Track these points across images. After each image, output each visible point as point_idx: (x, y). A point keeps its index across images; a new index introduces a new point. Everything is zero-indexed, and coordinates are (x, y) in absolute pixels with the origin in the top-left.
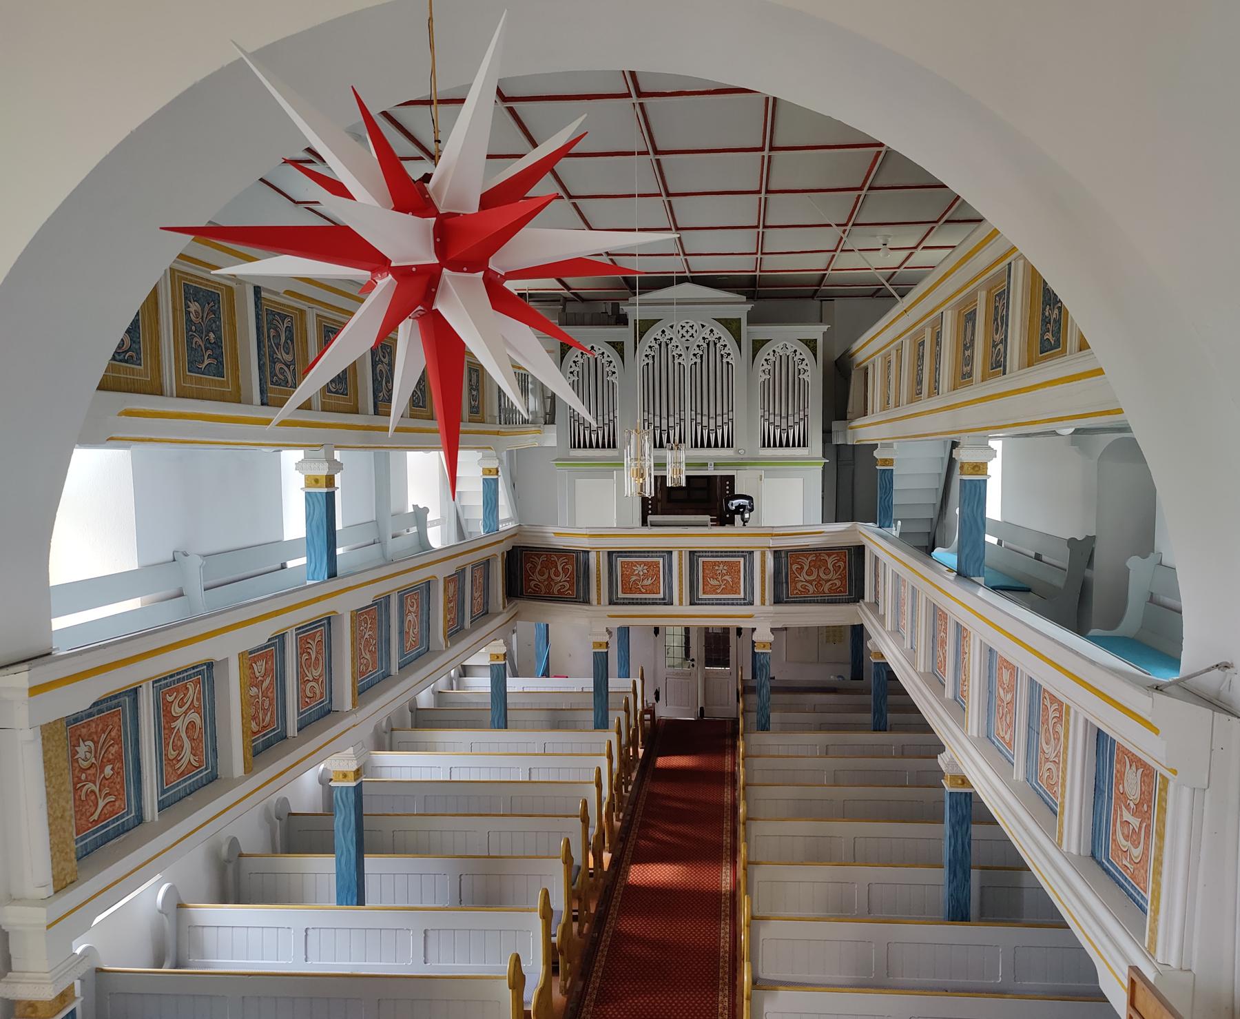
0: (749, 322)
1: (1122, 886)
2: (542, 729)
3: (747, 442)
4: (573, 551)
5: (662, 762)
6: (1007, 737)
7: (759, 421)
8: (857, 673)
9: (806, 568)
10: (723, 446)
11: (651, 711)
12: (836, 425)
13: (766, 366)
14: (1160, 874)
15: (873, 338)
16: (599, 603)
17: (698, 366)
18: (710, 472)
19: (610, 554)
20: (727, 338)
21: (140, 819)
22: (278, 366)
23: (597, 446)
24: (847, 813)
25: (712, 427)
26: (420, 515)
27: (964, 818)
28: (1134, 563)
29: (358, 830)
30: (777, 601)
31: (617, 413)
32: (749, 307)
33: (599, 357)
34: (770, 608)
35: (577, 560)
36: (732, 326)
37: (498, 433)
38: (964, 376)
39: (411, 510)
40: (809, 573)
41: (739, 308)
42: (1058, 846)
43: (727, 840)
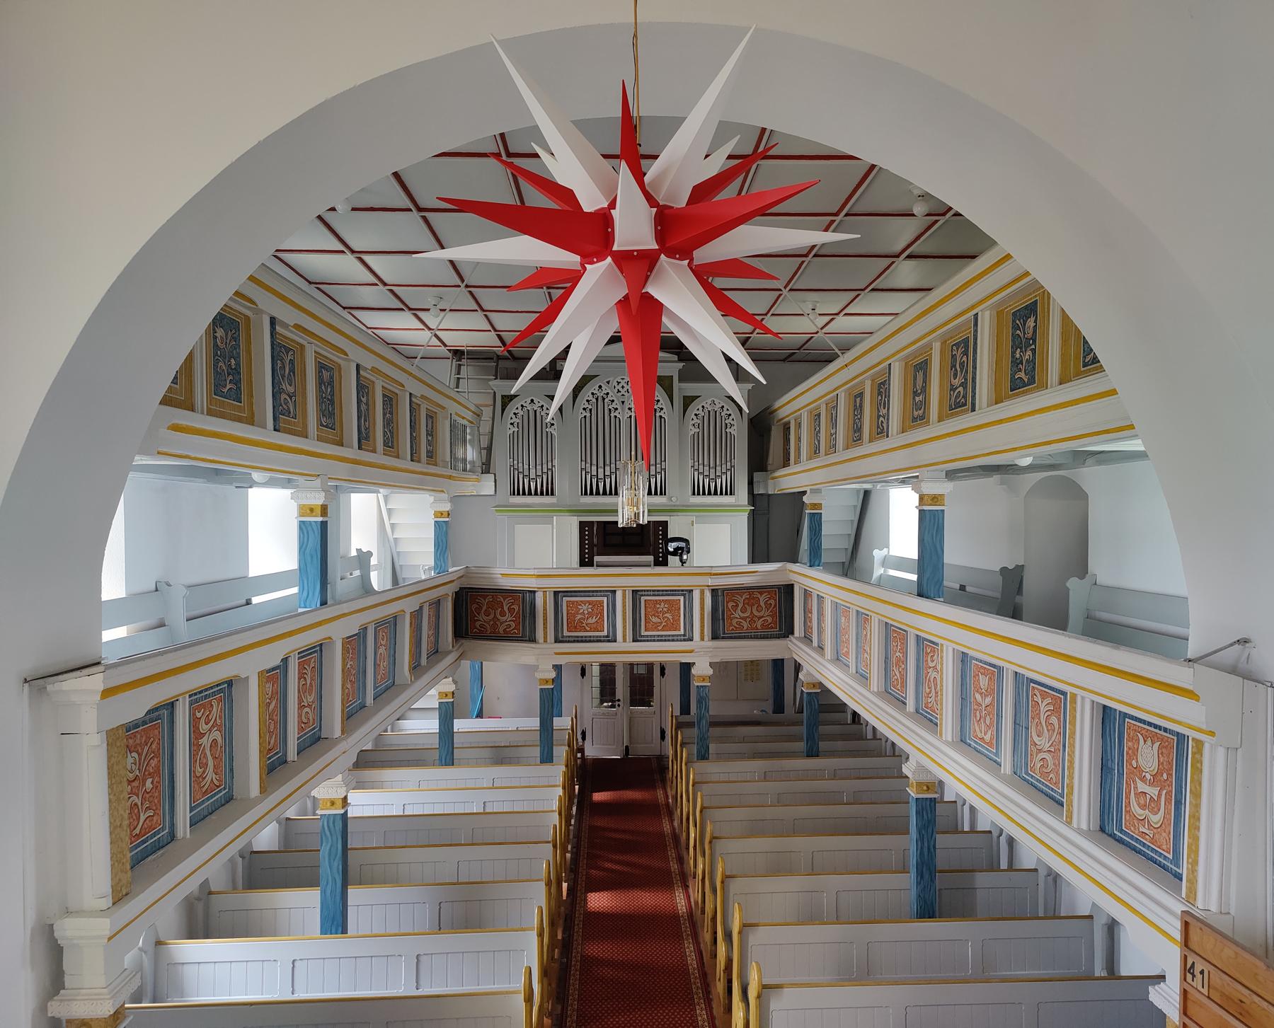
0: (681, 380)
1: (1139, 852)
2: (486, 765)
3: (679, 491)
5: (598, 797)
6: (987, 738)
7: (690, 471)
8: (779, 707)
9: (741, 605)
10: (656, 494)
11: (581, 750)
12: (757, 475)
14: (1198, 828)
15: (802, 394)
16: (545, 641)
21: (172, 836)
22: (284, 396)
23: (536, 494)
24: (796, 829)
26: (363, 558)
27: (929, 821)
28: (1073, 583)
29: (333, 864)
30: (715, 637)
31: (556, 462)
32: (681, 365)
33: (539, 410)
34: (709, 643)
35: (523, 601)
37: (450, 477)
38: (914, 419)
39: (354, 553)
42: (1069, 822)
43: (674, 866)
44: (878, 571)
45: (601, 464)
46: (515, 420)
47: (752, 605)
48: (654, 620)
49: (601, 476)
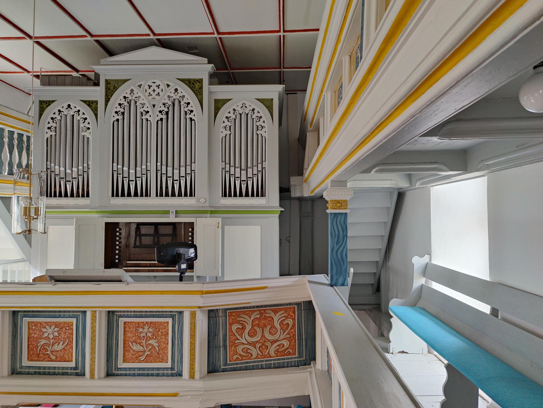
0: (211, 84)
3: (207, 192)
9: (248, 328)
12: (294, 180)
13: (227, 123)
17: (164, 121)
19: (15, 314)
25: (176, 177)
36: (195, 85)
40: (252, 334)
41: (202, 69)
44: (419, 281)
46: (52, 124)
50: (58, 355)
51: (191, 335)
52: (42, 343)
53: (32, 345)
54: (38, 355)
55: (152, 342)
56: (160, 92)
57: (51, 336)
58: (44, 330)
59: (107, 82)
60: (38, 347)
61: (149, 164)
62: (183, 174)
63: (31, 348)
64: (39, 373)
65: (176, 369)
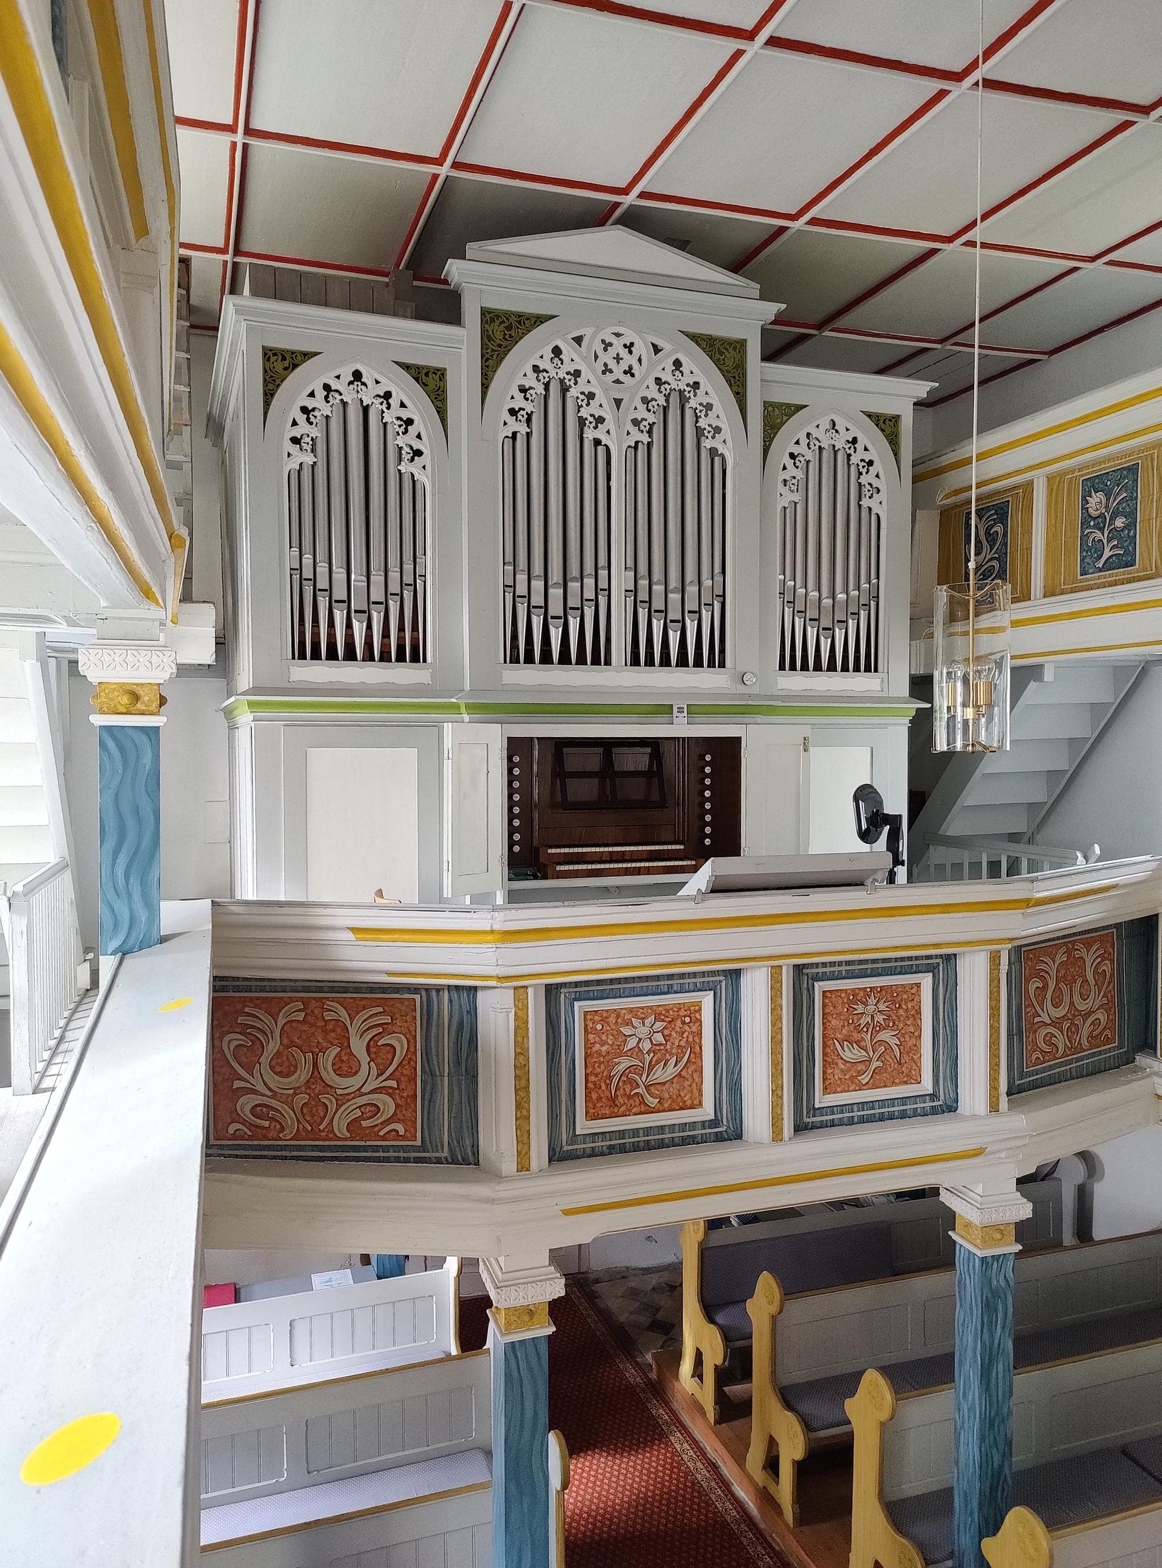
4: (415, 989)
9: (1052, 985)
16: (523, 1166)
18: (681, 728)
19: (552, 991)
20: (713, 388)
32: (772, 309)
33: (377, 406)
41: (746, 314)
45: (556, 575)
47: (1071, 983)
48: (851, 1054)
49: (556, 608)
50: (666, 1095)
51: (991, 1008)
52: (622, 1067)
53: (596, 1076)
54: (613, 1100)
55: (885, 1035)
56: (636, 365)
57: (646, 1046)
58: (627, 1031)
59: (489, 316)
60: (611, 1078)
61: (603, 573)
62: (573, 602)
63: (594, 1083)
64: (623, 1149)
65: (942, 1097)
